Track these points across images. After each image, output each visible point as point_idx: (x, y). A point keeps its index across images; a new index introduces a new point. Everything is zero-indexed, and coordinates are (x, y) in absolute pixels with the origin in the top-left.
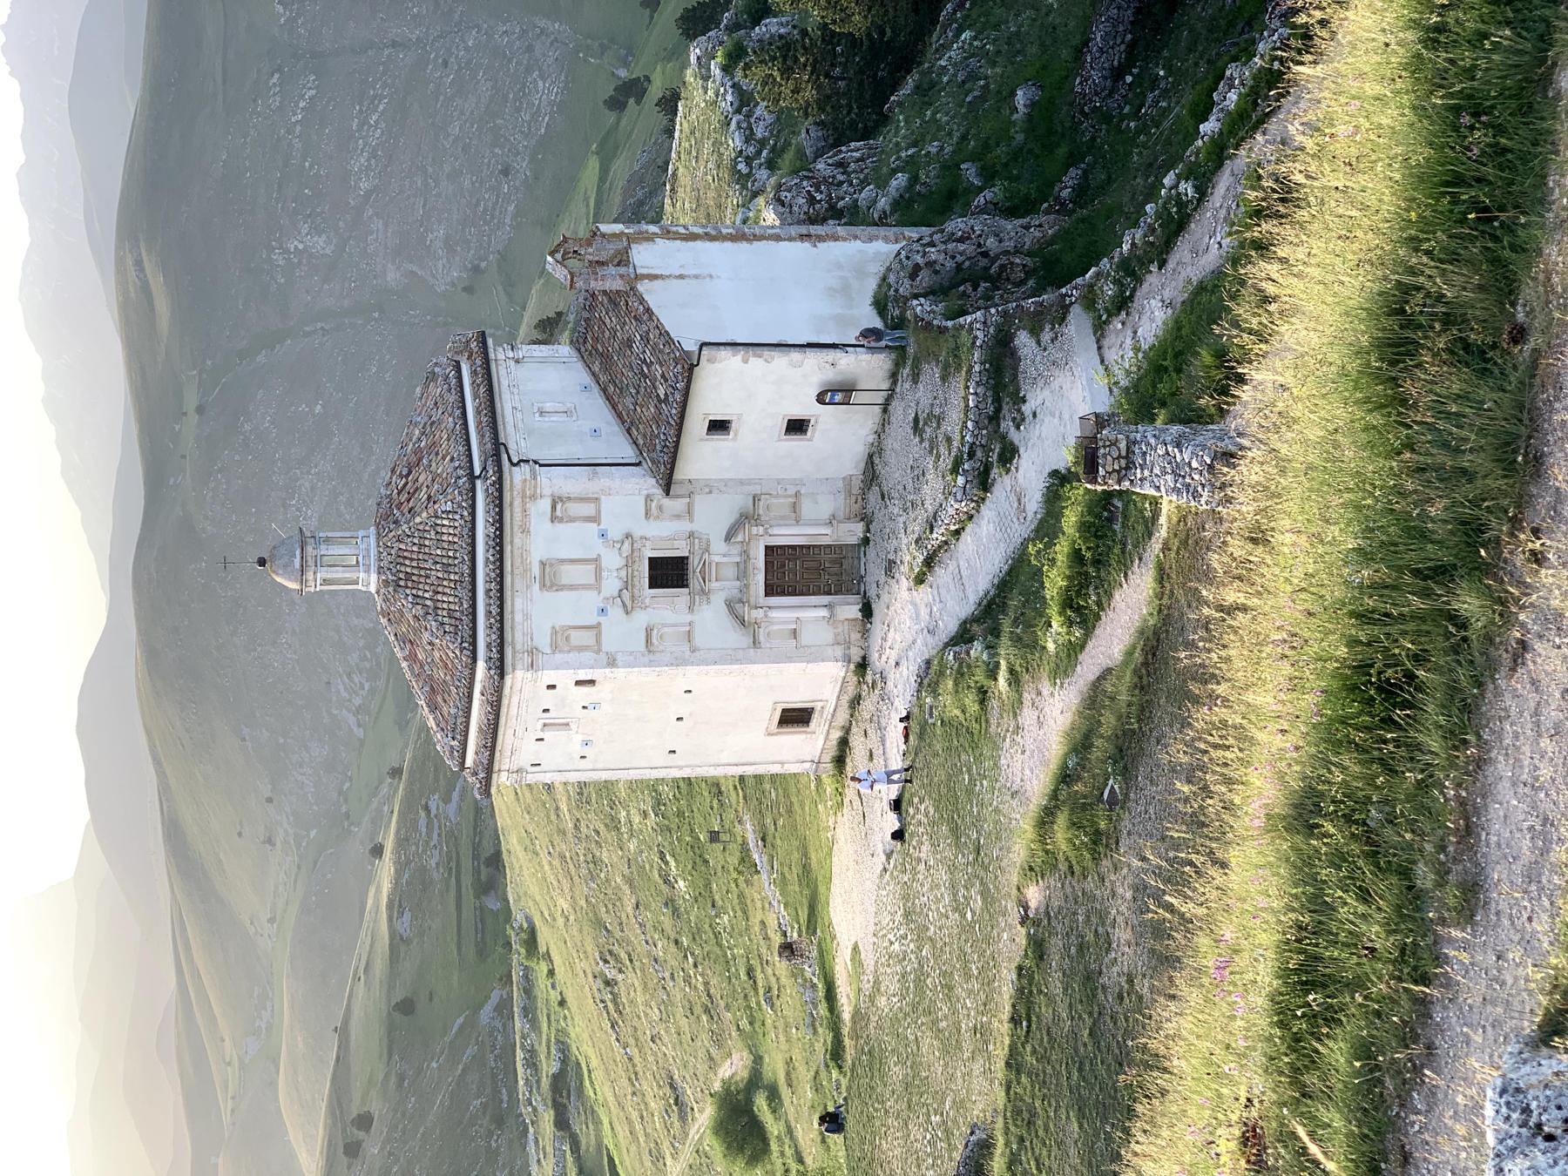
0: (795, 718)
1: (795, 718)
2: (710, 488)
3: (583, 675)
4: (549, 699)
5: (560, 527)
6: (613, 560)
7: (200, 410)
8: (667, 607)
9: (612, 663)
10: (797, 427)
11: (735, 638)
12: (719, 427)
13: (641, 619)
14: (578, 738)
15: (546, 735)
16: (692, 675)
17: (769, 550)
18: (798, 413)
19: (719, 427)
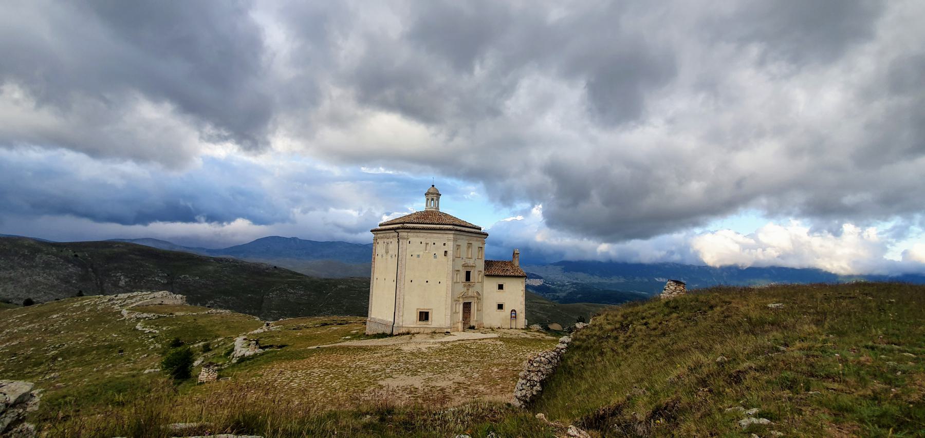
0: (424, 316)
1: (424, 316)
2: (482, 287)
3: (450, 253)
4: (439, 244)
5: (477, 250)
6: (471, 262)
7: (76, 256)
8: (463, 276)
9: (453, 260)
10: (500, 307)
11: (457, 295)
12: (501, 287)
13: (461, 268)
14: (421, 253)
15: (423, 244)
16: (446, 283)
17: (470, 303)
18: (505, 307)
19: (501, 287)
